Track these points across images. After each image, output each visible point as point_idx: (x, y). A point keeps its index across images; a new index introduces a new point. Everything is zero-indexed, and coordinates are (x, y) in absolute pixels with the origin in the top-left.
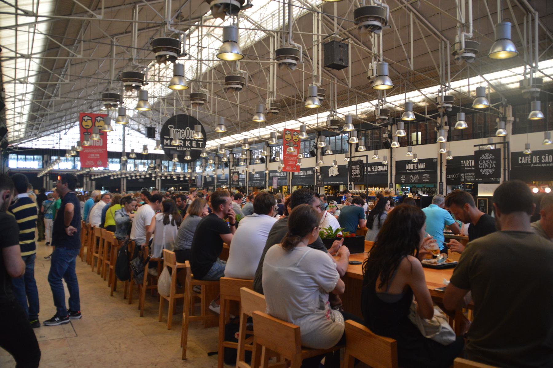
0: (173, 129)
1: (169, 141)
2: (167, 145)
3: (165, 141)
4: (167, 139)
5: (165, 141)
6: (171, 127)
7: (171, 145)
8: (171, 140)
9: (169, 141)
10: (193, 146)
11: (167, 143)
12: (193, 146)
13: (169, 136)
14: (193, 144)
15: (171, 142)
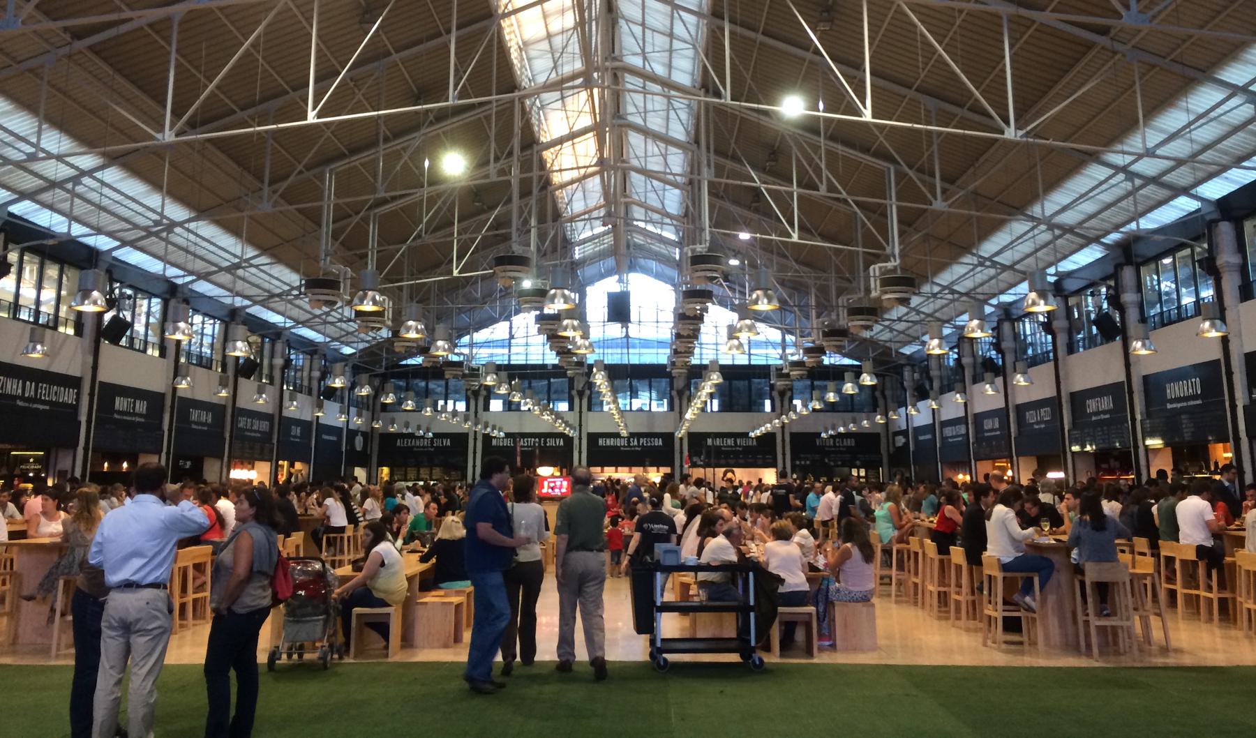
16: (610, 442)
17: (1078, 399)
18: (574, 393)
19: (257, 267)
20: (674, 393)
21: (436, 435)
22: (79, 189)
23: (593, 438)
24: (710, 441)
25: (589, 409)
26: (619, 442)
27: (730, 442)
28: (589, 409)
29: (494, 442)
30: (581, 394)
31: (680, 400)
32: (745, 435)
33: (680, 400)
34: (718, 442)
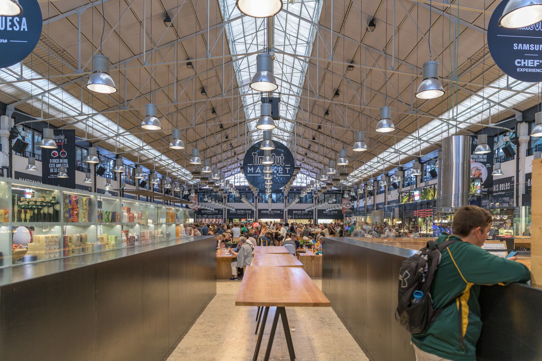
0: (256, 156)
1: (252, 168)
2: (251, 173)
3: (249, 168)
4: (250, 167)
5: (249, 168)
6: (255, 155)
7: (254, 173)
8: (255, 167)
9: (252, 168)
10: (279, 172)
11: (250, 170)
12: (279, 172)
13: (253, 164)
14: (279, 170)
15: (255, 170)
16: (265, 212)
17: (377, 205)
18: (254, 197)
19: (164, 161)
20: (284, 198)
21: (215, 209)
22: (118, 139)
23: (260, 211)
24: (294, 212)
25: (259, 202)
26: (267, 212)
27: (300, 212)
28: (259, 202)
29: (231, 212)
30: (256, 198)
31: (286, 199)
32: (304, 210)
33: (286, 199)
34: (296, 212)
